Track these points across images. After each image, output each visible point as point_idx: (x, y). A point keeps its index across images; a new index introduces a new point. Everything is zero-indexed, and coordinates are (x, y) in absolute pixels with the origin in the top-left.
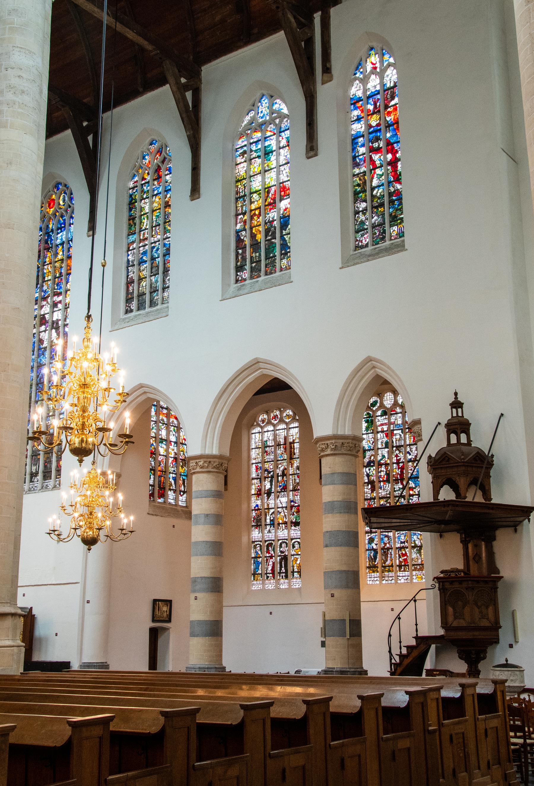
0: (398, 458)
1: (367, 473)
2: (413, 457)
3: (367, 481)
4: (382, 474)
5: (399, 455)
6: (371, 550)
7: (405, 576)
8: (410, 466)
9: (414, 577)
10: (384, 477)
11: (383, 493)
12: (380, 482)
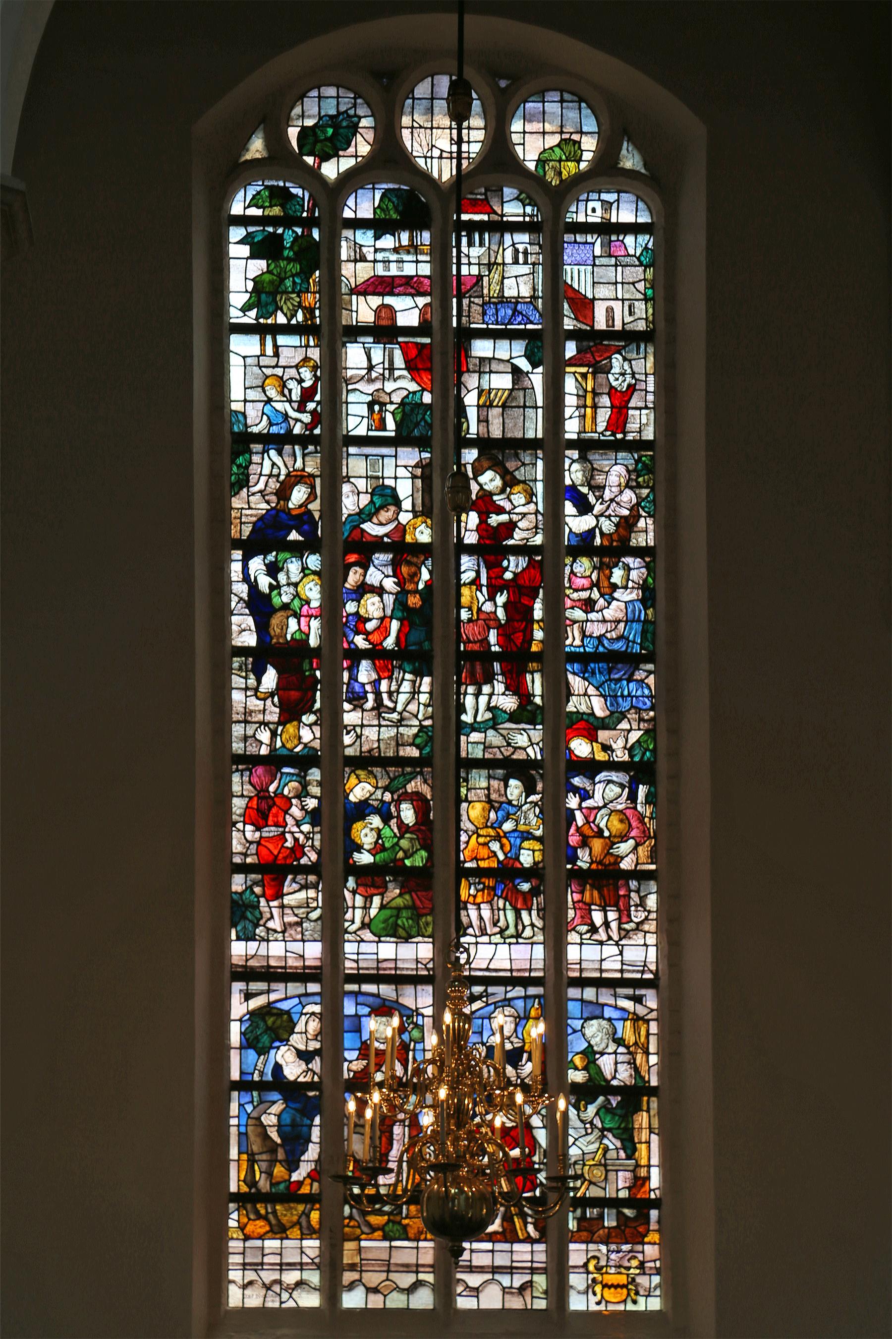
0: (494, 520)
1: (253, 587)
2: (607, 526)
3: (250, 640)
4: (372, 606)
5: (500, 500)
6: (262, 1086)
7: (511, 1270)
8: (579, 582)
9: (577, 1280)
10: (383, 629)
11: (371, 734)
12: (356, 656)
